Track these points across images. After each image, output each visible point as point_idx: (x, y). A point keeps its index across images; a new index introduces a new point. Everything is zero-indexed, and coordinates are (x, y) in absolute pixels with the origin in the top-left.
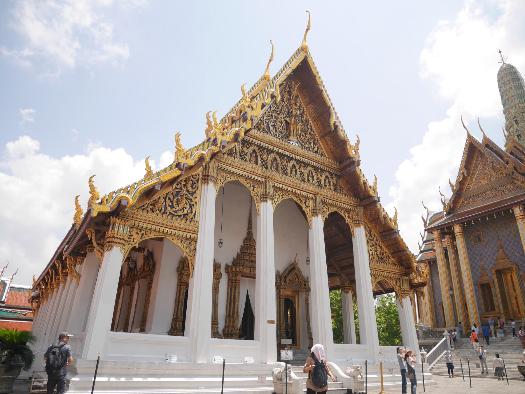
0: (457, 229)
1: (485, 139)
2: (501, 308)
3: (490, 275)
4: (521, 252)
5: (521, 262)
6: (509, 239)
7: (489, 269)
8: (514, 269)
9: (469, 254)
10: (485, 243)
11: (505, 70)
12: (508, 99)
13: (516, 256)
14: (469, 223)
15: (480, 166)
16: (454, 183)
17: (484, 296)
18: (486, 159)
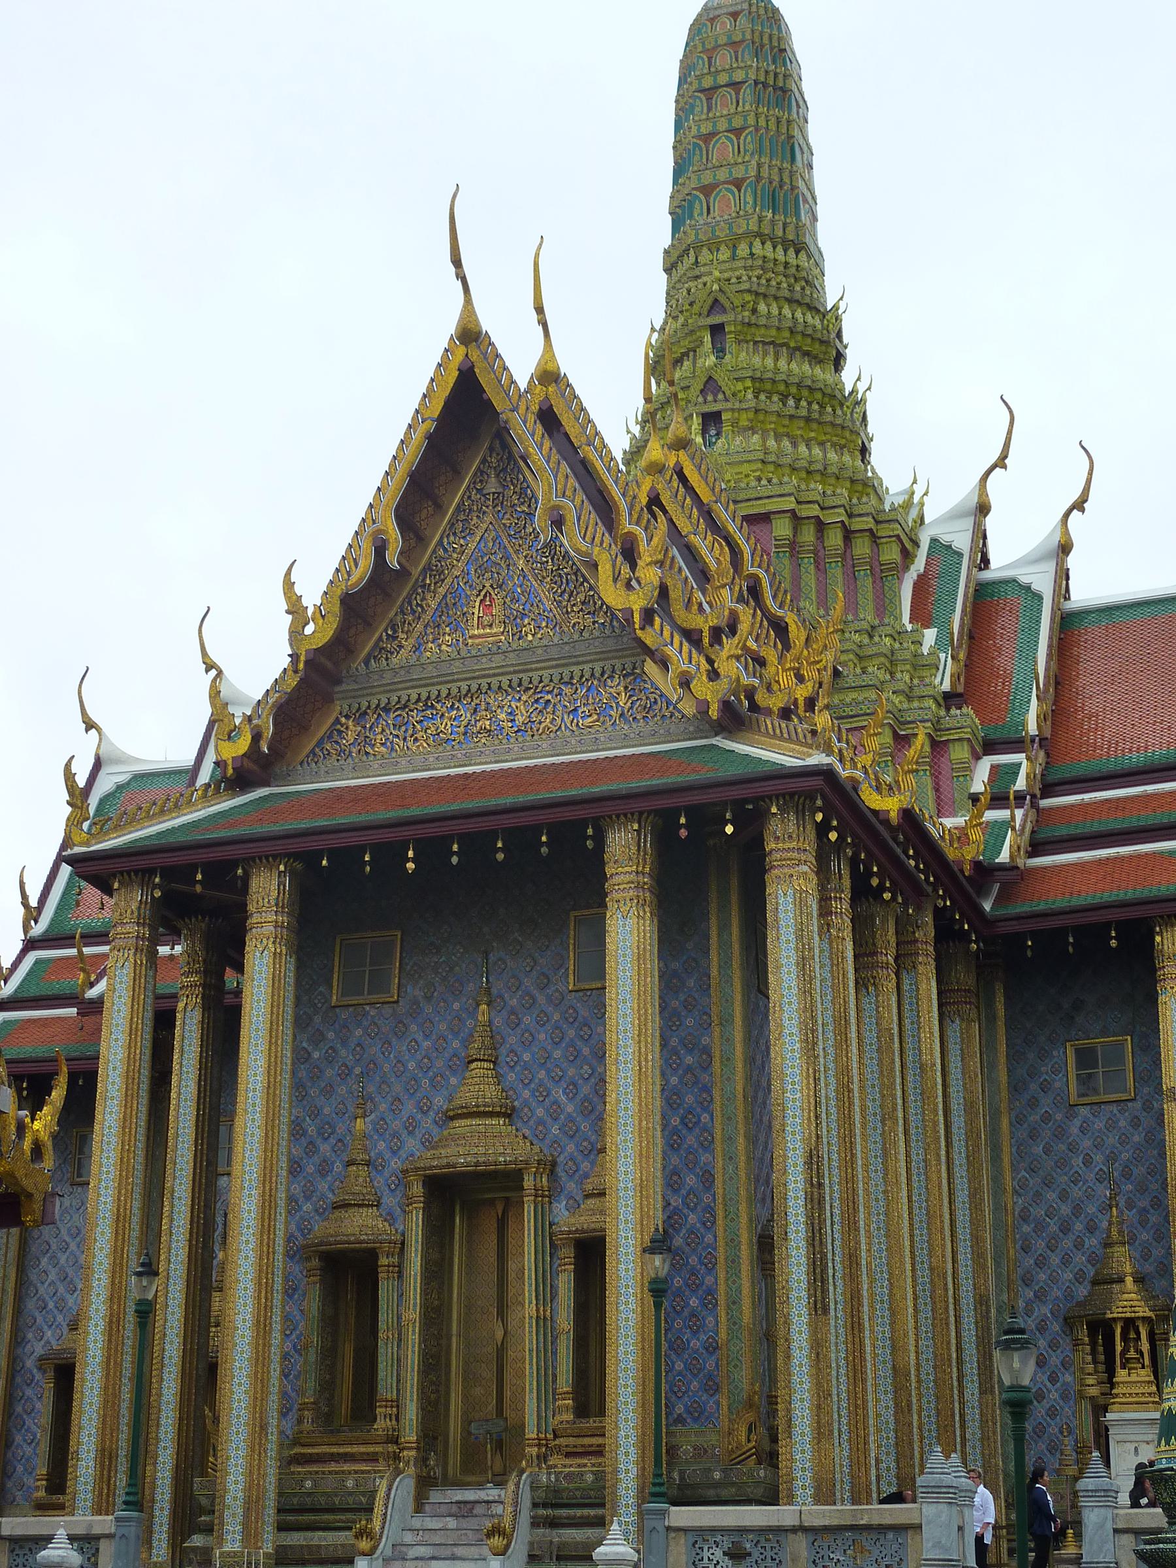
0: (267, 894)
1: (549, 376)
2: (412, 1411)
3: (389, 1201)
4: (585, 1090)
6: (541, 999)
7: (395, 1164)
8: (528, 1182)
9: (301, 1057)
10: (402, 1008)
11: (735, 15)
12: (707, 190)
13: (555, 1111)
14: (346, 857)
15: (482, 525)
16: (312, 595)
17: (330, 1323)
18: (527, 496)
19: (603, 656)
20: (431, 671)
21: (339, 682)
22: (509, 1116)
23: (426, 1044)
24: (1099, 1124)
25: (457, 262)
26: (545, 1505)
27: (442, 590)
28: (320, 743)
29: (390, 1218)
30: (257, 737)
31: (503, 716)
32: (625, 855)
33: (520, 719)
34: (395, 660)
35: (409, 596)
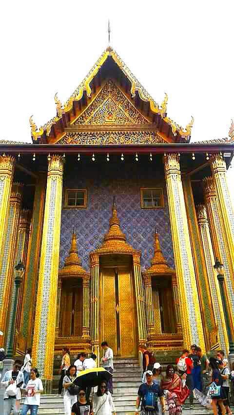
5: (145, 251)
7: (87, 253)
10: (88, 210)
19: (145, 129)
22: (125, 241)
23: (96, 220)
25: (109, 32)
27: (96, 110)
35: (87, 109)
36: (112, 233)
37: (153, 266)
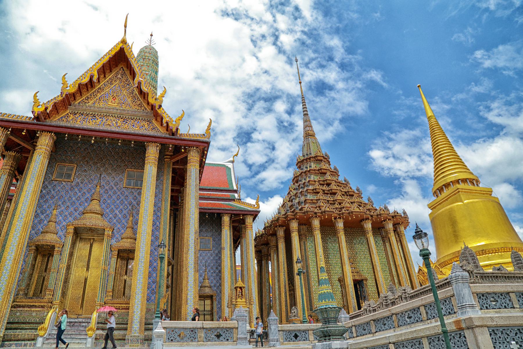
0: (45, 143)
3: (61, 233)
6: (115, 188)
7: (64, 223)
10: (73, 184)
20: (96, 109)
21: (70, 105)
24: (204, 255)
25: (125, 27)
26: (101, 323)
27: (102, 93)
28: (62, 118)
29: (60, 237)
30: (46, 109)
31: (114, 122)
32: (152, 153)
33: (118, 124)
34: (87, 105)
36: (88, 208)
37: (124, 240)
